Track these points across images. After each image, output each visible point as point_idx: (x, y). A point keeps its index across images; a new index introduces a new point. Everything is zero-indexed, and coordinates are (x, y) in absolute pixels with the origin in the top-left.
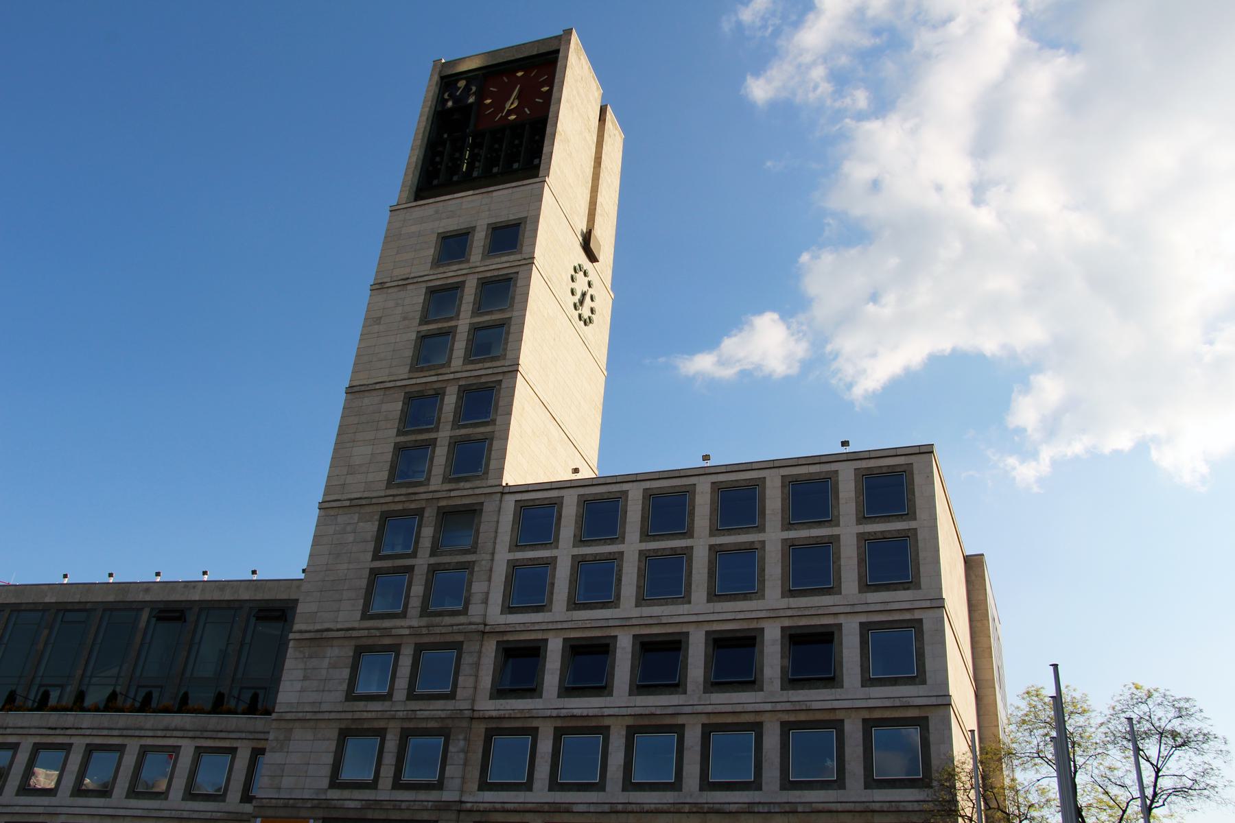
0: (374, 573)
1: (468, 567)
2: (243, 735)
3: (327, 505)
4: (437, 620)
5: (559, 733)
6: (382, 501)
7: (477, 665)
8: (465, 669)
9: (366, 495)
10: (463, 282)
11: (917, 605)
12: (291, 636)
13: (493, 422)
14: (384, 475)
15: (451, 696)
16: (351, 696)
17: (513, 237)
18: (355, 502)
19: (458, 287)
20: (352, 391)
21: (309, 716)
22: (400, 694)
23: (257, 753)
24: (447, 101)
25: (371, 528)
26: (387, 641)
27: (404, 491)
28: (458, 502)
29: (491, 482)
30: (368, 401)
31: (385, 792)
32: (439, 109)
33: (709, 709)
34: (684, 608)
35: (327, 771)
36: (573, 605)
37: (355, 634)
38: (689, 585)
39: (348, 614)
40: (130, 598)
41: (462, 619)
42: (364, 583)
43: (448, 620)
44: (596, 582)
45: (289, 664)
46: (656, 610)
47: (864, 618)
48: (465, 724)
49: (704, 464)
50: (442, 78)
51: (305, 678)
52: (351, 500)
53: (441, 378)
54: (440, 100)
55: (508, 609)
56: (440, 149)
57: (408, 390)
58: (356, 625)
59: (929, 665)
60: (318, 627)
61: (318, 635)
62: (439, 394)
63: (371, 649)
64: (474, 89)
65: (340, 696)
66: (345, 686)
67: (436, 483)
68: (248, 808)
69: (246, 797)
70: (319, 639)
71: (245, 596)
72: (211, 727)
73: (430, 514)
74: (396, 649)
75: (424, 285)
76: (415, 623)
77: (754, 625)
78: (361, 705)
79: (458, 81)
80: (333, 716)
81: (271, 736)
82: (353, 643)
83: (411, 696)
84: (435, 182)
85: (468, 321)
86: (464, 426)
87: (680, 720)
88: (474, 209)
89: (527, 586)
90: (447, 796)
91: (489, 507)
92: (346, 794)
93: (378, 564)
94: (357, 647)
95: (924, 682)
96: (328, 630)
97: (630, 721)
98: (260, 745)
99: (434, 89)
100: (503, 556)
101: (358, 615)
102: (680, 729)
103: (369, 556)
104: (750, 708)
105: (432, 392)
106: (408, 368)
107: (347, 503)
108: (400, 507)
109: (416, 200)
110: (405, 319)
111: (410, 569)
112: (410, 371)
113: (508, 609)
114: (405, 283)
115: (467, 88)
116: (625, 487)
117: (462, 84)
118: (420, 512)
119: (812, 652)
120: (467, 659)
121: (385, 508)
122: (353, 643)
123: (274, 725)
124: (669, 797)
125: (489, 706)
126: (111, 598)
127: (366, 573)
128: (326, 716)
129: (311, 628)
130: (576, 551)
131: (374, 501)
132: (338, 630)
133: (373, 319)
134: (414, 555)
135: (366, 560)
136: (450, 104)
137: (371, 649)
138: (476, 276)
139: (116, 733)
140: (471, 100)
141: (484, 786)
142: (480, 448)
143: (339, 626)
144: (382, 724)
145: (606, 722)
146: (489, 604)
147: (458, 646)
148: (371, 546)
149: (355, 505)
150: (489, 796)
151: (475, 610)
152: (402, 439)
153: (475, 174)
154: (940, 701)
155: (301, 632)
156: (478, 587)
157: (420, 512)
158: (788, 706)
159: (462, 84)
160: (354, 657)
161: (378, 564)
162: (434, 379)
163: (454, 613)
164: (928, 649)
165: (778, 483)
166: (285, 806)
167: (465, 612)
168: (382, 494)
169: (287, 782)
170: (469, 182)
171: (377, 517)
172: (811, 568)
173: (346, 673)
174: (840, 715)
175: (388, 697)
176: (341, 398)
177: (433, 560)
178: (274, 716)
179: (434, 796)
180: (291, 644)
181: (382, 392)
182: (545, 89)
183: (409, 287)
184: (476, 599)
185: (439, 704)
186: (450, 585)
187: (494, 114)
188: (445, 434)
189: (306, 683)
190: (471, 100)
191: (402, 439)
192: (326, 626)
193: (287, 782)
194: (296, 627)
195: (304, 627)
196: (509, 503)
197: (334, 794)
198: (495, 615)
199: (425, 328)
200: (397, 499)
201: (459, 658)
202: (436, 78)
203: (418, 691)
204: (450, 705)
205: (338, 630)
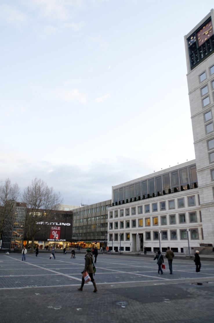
2: (195, 193)
3: (195, 143)
6: (206, 138)
9: (202, 138)
10: (207, 84)
12: (197, 171)
14: (205, 132)
18: (200, 140)
20: (192, 118)
21: (205, 186)
23: (198, 195)
24: (190, 44)
25: (205, 144)
27: (210, 134)
30: (196, 118)
32: (189, 47)
37: (209, 167)
40: (166, 172)
42: (207, 156)
45: (198, 177)
50: (187, 39)
51: (202, 179)
52: (199, 140)
53: (209, 107)
54: (189, 44)
56: (192, 56)
57: (203, 112)
58: (209, 165)
60: (201, 168)
61: (202, 170)
64: (195, 38)
66: (210, 178)
68: (200, 206)
69: (199, 204)
70: (202, 170)
71: (187, 165)
72: (188, 192)
75: (199, 88)
79: (190, 38)
80: (210, 185)
81: (199, 192)
82: (209, 169)
84: (194, 64)
85: (211, 92)
93: (209, 151)
94: (211, 170)
96: (204, 168)
98: (198, 194)
99: (187, 43)
101: (208, 163)
103: (207, 150)
105: (209, 111)
106: (202, 108)
107: (199, 141)
108: (210, 138)
109: (191, 70)
110: (198, 97)
112: (203, 108)
121: (207, 139)
122: (209, 169)
123: (199, 189)
126: (163, 173)
127: (207, 154)
128: (209, 185)
129: (200, 168)
131: (204, 139)
132: (206, 167)
133: (191, 101)
138: (210, 81)
139: (172, 197)
140: (195, 41)
143: (206, 167)
148: (207, 148)
149: (201, 141)
152: (206, 123)
153: (202, 57)
155: (198, 170)
159: (192, 38)
160: (211, 172)
162: (208, 108)
166: (206, 205)
168: (205, 136)
169: (205, 200)
170: (202, 60)
171: (206, 142)
176: (190, 120)
178: (198, 188)
180: (197, 173)
181: (198, 115)
182: (211, 28)
183: (196, 90)
187: (201, 41)
189: (204, 179)
191: (206, 123)
192: (203, 167)
193: (205, 200)
194: (197, 169)
195: (199, 169)
200: (209, 137)
202: (186, 40)
205: (206, 167)
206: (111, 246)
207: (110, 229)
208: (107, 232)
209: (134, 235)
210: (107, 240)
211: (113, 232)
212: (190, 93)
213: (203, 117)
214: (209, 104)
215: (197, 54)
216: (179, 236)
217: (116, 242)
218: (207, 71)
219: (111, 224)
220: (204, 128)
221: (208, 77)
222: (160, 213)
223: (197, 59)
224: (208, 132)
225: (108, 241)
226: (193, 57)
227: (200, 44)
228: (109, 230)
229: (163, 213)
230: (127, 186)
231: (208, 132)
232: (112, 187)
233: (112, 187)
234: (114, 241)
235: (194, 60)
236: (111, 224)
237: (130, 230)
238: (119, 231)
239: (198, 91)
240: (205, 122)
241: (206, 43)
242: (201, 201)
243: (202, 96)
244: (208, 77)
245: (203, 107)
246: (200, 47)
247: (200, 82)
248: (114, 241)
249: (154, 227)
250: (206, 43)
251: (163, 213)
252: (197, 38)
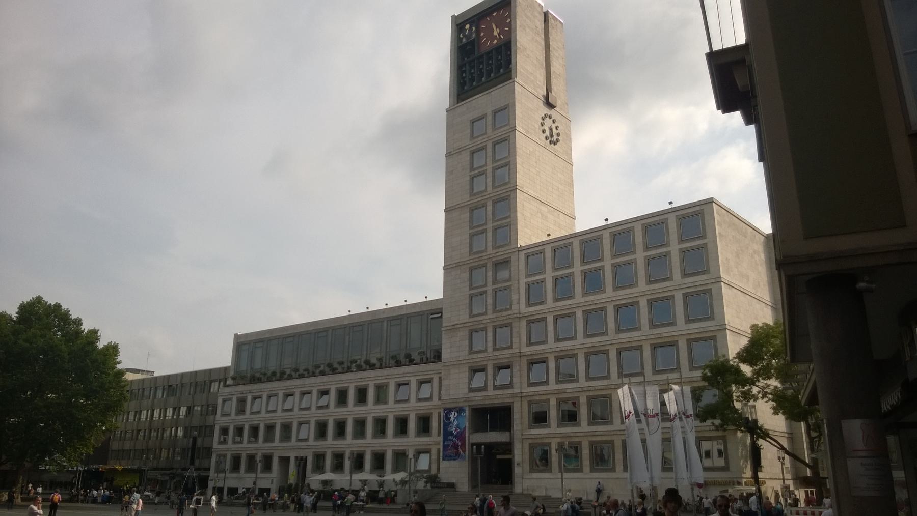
0: (471, 297)
1: (508, 288)
4: (499, 314)
5: (557, 359)
7: (519, 333)
8: (514, 335)
11: (708, 282)
13: (509, 217)
14: (468, 250)
15: (511, 347)
16: (471, 352)
17: (506, 111)
19: (484, 148)
20: (447, 211)
22: (490, 349)
25: (466, 275)
26: (481, 326)
28: (500, 258)
29: (514, 246)
31: (490, 392)
33: (619, 341)
34: (603, 296)
35: (466, 386)
36: (556, 299)
38: (604, 284)
39: (464, 317)
41: (510, 312)
42: (467, 301)
43: (504, 313)
44: (563, 288)
45: (444, 341)
46: (591, 298)
47: (684, 291)
48: (518, 359)
49: (605, 223)
55: (529, 305)
59: (716, 311)
62: (484, 206)
63: (476, 331)
65: (466, 352)
67: (490, 250)
68: (440, 403)
70: (454, 329)
73: (489, 265)
74: (484, 329)
76: (491, 317)
77: (634, 300)
78: (475, 356)
83: (495, 349)
86: (498, 220)
87: (607, 348)
88: (484, 102)
89: (534, 294)
90: (516, 390)
91: (514, 258)
92: (476, 394)
93: (472, 292)
95: (713, 319)
97: (586, 350)
100: (523, 281)
101: (468, 316)
102: (606, 352)
103: (468, 288)
104: (635, 339)
111: (485, 292)
113: (529, 305)
114: (460, 151)
115: (470, 28)
116: (571, 240)
117: (467, 27)
118: (485, 266)
119: (660, 307)
120: (515, 330)
124: (605, 382)
125: (526, 350)
130: (554, 274)
134: (485, 285)
135: (466, 291)
136: (464, 40)
137: (476, 331)
141: (530, 385)
142: (506, 223)
144: (485, 363)
145: (576, 352)
146: (520, 305)
147: (509, 325)
148: (467, 284)
149: (458, 265)
150: (532, 389)
151: (515, 307)
154: (722, 327)
156: (515, 297)
157: (485, 266)
158: (653, 337)
159: (467, 27)
161: (472, 292)
163: (506, 310)
164: (715, 303)
165: (640, 228)
167: (510, 309)
172: (657, 268)
173: (467, 342)
174: (676, 339)
175: (485, 351)
176: (442, 215)
177: (494, 287)
179: (509, 391)
182: (508, 21)
184: (514, 302)
185: (506, 351)
186: (503, 292)
188: (490, 226)
189: (453, 348)
190: (474, 36)
194: (444, 325)
196: (522, 255)
197: (471, 395)
198: (524, 309)
199: (473, 173)
201: (511, 330)
202: (455, 26)
203: (498, 346)
204: (511, 351)
206: (221, 486)
207: (220, 443)
208: (209, 451)
209: (285, 461)
210: (209, 469)
211: (228, 450)
212: (449, 155)
213: (468, 215)
214: (482, 192)
215: (473, 67)
216: (389, 465)
217: (234, 475)
218: (489, 118)
219: (225, 431)
220: (468, 241)
221: (489, 131)
222: (351, 411)
223: (472, 80)
224: (474, 250)
225: (212, 474)
226: (465, 71)
227: (483, 50)
228: (215, 445)
229: (361, 411)
230: (277, 338)
231: (474, 250)
232: (236, 335)
233: (236, 335)
234: (228, 475)
235: (467, 80)
236: (225, 431)
237: (276, 448)
238: (246, 447)
239: (466, 156)
240: (471, 228)
241: (494, 52)
242: (443, 393)
243: (472, 169)
244: (489, 131)
245: (472, 194)
246: (482, 56)
247: (472, 137)
248: (228, 475)
249: (335, 442)
250: (494, 52)
251: (361, 411)
252: (478, 32)
